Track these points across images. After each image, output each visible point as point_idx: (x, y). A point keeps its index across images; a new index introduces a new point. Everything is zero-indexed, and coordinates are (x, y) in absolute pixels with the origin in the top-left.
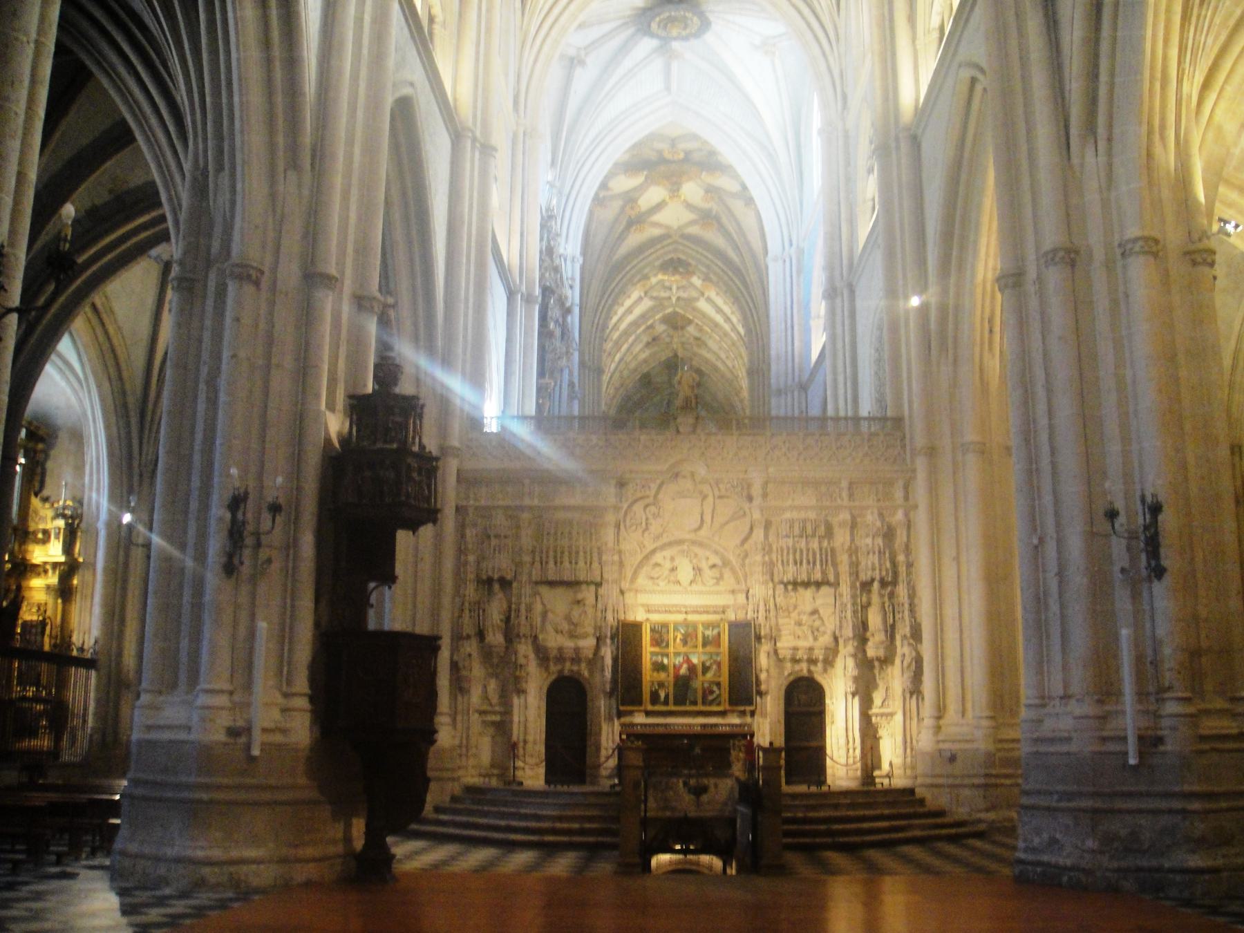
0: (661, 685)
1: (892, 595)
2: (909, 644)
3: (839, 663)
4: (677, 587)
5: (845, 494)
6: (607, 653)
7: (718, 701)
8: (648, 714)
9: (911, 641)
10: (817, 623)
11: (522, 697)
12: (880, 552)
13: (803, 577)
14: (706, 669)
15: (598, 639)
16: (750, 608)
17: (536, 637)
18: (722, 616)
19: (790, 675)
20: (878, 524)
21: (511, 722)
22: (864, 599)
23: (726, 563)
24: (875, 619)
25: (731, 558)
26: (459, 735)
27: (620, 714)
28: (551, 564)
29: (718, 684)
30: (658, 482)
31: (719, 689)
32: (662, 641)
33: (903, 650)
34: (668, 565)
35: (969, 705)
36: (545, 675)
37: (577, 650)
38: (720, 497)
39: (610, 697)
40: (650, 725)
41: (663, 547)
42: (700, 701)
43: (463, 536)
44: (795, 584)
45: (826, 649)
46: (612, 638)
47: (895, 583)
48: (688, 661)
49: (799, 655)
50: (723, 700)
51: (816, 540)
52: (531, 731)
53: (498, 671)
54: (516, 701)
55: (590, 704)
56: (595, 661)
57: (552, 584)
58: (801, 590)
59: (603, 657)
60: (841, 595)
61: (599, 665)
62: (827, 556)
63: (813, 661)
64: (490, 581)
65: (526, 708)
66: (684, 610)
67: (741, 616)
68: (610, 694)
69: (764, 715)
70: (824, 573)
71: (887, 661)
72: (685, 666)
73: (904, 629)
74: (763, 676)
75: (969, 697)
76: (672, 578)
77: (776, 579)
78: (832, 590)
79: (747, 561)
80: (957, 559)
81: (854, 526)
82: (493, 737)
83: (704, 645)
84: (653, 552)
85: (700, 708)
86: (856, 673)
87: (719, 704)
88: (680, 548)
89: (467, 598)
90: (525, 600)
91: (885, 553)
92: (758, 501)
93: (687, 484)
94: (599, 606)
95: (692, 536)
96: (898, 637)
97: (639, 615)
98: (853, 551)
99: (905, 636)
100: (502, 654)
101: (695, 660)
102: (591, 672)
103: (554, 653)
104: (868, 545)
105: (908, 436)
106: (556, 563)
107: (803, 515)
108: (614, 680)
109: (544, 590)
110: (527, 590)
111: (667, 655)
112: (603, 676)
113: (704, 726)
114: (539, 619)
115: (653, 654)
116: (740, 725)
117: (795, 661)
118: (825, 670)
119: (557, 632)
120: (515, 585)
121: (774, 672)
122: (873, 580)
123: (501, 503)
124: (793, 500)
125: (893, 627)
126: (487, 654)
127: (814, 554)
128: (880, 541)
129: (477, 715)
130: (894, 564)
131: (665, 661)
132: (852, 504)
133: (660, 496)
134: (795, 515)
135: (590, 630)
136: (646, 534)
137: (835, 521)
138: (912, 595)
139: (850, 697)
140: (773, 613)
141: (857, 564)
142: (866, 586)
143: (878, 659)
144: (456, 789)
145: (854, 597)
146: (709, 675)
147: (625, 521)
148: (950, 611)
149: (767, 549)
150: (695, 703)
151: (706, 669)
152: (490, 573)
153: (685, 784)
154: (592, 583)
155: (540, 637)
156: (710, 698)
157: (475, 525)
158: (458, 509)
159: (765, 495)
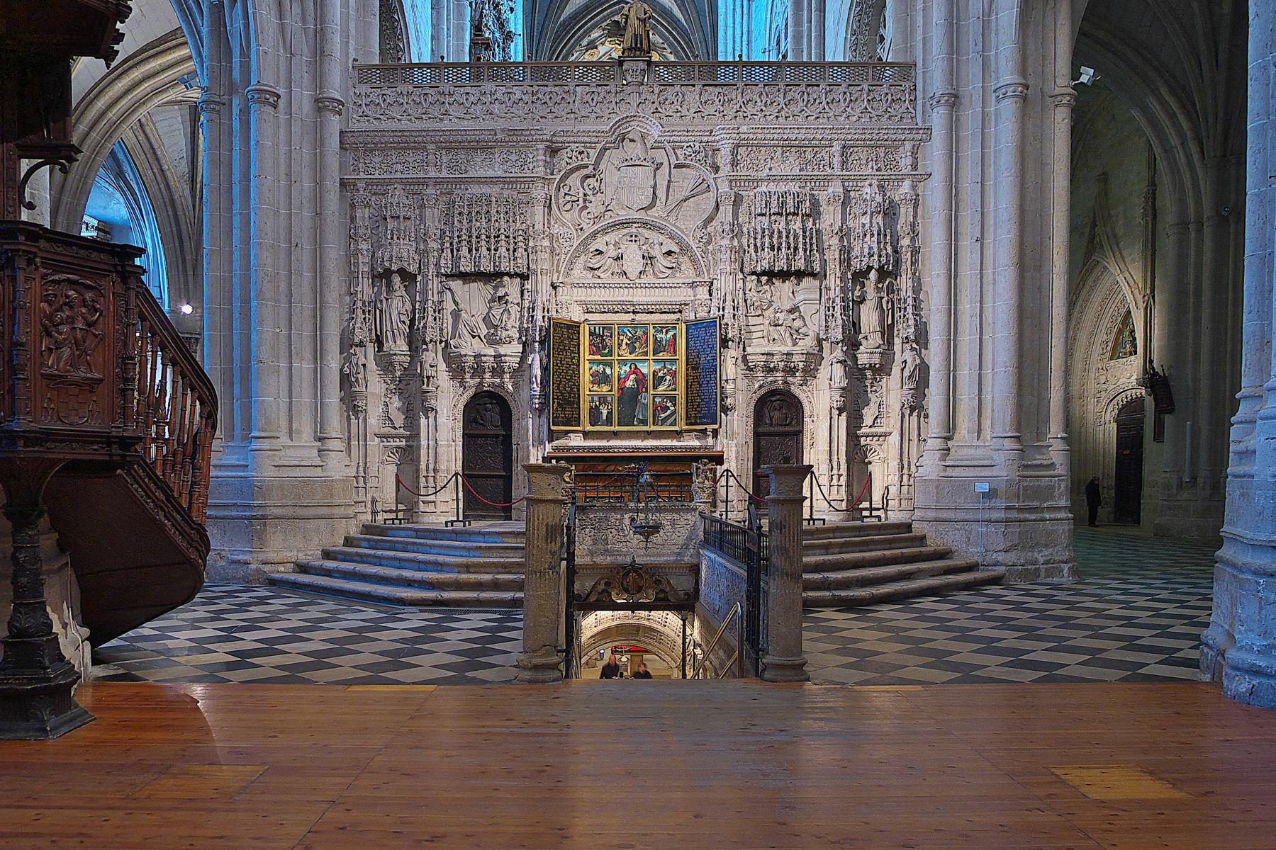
0: (603, 399)
1: (891, 290)
2: (912, 349)
3: (824, 372)
4: (624, 280)
5: (837, 161)
6: (535, 361)
8: (586, 435)
9: (914, 345)
10: (798, 323)
12: (879, 235)
13: (781, 265)
14: (658, 381)
15: (524, 344)
16: (715, 303)
18: (678, 315)
19: (761, 387)
20: (879, 199)
21: (419, 447)
22: (857, 293)
23: (685, 249)
24: (869, 318)
25: (691, 243)
26: (354, 464)
27: (552, 436)
28: (465, 251)
29: (673, 399)
30: (599, 146)
31: (674, 405)
33: (903, 355)
34: (613, 253)
35: (987, 423)
37: (498, 356)
38: (677, 166)
40: (589, 448)
41: (605, 231)
43: (353, 219)
44: (771, 275)
46: (541, 343)
47: (895, 274)
48: (636, 371)
49: (775, 361)
51: (799, 218)
52: (443, 457)
53: (401, 386)
54: (423, 421)
56: (522, 370)
57: (465, 277)
58: (777, 283)
60: (828, 289)
61: (526, 378)
62: (811, 238)
63: (791, 371)
64: (387, 274)
66: (632, 309)
67: (702, 314)
68: (540, 411)
70: (807, 260)
71: (881, 370)
72: (632, 377)
73: (905, 329)
74: (729, 388)
75: (987, 413)
76: (617, 270)
77: (747, 270)
78: (817, 283)
79: (710, 247)
80: (981, 240)
81: (845, 203)
84: (594, 235)
86: (844, 384)
88: (627, 231)
89: (359, 296)
90: (433, 297)
91: (885, 235)
92: (725, 170)
93: (634, 150)
94: (526, 304)
95: (641, 216)
96: (897, 341)
97: (576, 315)
98: (844, 234)
99: (906, 338)
100: (406, 365)
101: (645, 371)
103: (470, 361)
104: (864, 225)
105: (920, 86)
106: (470, 251)
107: (782, 188)
109: (456, 285)
110: (434, 285)
114: (450, 321)
116: (700, 448)
118: (804, 383)
119: (474, 337)
120: (419, 278)
121: (742, 384)
122: (870, 268)
123: (399, 175)
124: (770, 169)
125: (891, 327)
126: (386, 364)
127: (796, 236)
128: (879, 219)
130: (896, 251)
131: (608, 371)
132: (844, 173)
133: (602, 167)
134: (772, 187)
136: (586, 212)
137: (822, 197)
138: (917, 289)
139: (835, 412)
140: (742, 310)
141: (850, 249)
142: (860, 276)
143: (872, 367)
144: (354, 531)
145: (843, 290)
146: (661, 388)
147: (557, 199)
148: (967, 306)
149: (735, 231)
150: (644, 422)
152: (387, 264)
153: (633, 520)
154: (517, 275)
156: (663, 415)
157: (367, 205)
158: (343, 184)
159: (734, 163)
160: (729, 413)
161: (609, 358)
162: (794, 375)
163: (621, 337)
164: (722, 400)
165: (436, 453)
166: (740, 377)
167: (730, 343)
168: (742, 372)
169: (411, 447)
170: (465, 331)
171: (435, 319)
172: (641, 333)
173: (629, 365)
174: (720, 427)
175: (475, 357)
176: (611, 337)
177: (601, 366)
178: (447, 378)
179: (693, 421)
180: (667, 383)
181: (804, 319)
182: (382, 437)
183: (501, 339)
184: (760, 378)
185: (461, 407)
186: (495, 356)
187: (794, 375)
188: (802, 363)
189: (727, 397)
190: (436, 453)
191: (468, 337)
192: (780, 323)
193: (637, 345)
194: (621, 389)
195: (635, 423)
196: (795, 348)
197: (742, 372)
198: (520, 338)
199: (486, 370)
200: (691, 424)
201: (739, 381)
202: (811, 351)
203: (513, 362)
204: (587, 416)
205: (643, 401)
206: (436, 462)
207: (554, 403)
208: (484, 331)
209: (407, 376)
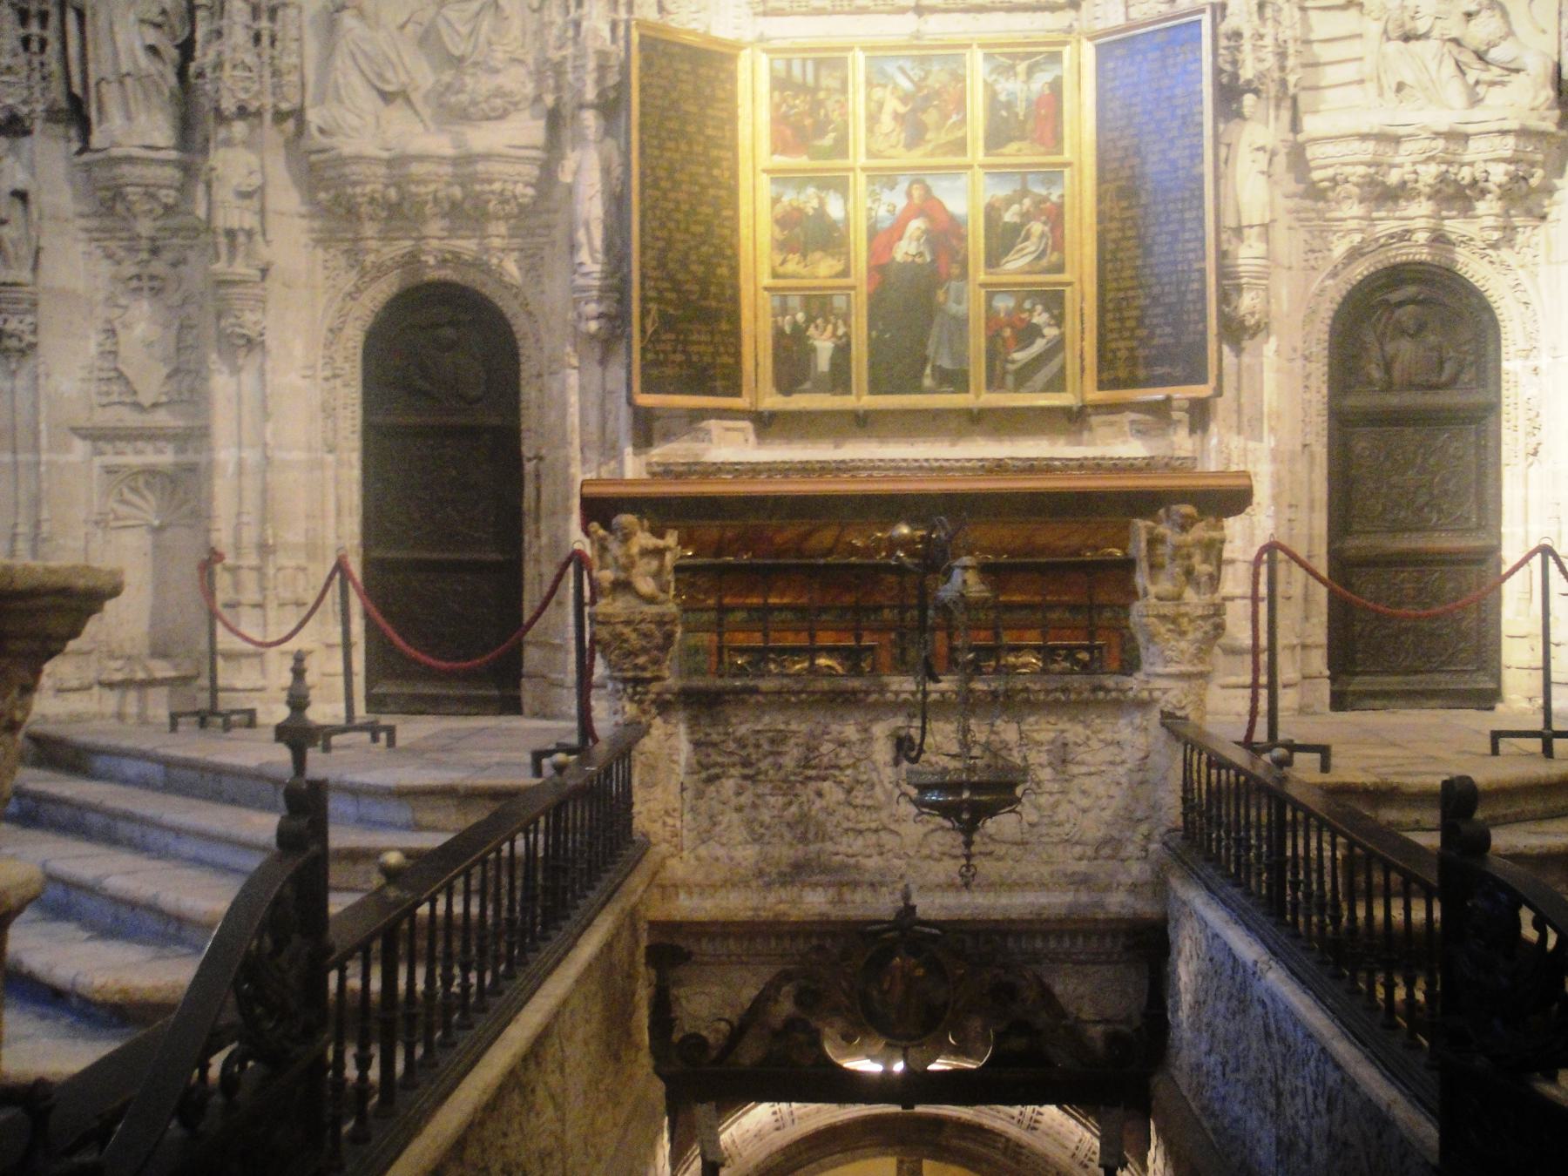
0: (819, 305)
7: (1053, 367)
8: (766, 424)
11: (250, 364)
15: (555, 120)
17: (298, 114)
19: (1355, 254)
27: (646, 429)
29: (1054, 301)
32: (821, 129)
36: (349, 280)
39: (603, 362)
42: (978, 371)
45: (1524, 133)
48: (928, 207)
50: (1072, 369)
53: (158, 267)
54: (221, 383)
55: (529, 393)
59: (570, 190)
61: (558, 234)
65: (265, 413)
69: (1248, 424)
72: (916, 225)
74: (1248, 255)
82: (157, 531)
83: (997, 137)
85: (980, 398)
87: (1057, 383)
102: (533, 263)
108: (615, 285)
111: (840, 185)
112: (576, 268)
113: (999, 467)
115: (781, 178)
116: (1148, 466)
117: (1385, 195)
118: (1508, 234)
119: (387, 97)
121: (1288, 244)
129: (80, 448)
131: (835, 209)
135: (518, 82)
146: (1015, 264)
150: (955, 380)
151: (1002, 239)
155: (313, 117)
156: (1020, 356)
160: (1247, 344)
161: (838, 163)
162: (1467, 211)
163: (878, 93)
164: (1224, 298)
165: (265, 492)
166: (1284, 220)
167: (1249, 100)
168: (1291, 204)
169: (192, 469)
170: (356, 80)
171: (257, 39)
172: (944, 77)
173: (903, 186)
174: (1219, 391)
175: (390, 163)
176: (844, 89)
177: (811, 191)
178: (305, 239)
179: (1122, 373)
180: (1031, 246)
181: (1505, 14)
182: (98, 436)
183: (474, 103)
184: (1353, 224)
185: (354, 336)
186: (455, 161)
187: (1467, 211)
188: (1503, 167)
189: (1239, 289)
190: (265, 492)
191: (366, 100)
192: (1422, 26)
193: (931, 117)
194: (880, 269)
195: (927, 382)
196: (1477, 114)
197: (1291, 204)
198: (538, 99)
199: (429, 209)
200: (1116, 384)
201: (1280, 234)
202: (1534, 123)
203: (519, 182)
204: (767, 363)
205: (953, 308)
206: (263, 521)
207: (645, 313)
208: (423, 75)
209: (175, 232)
